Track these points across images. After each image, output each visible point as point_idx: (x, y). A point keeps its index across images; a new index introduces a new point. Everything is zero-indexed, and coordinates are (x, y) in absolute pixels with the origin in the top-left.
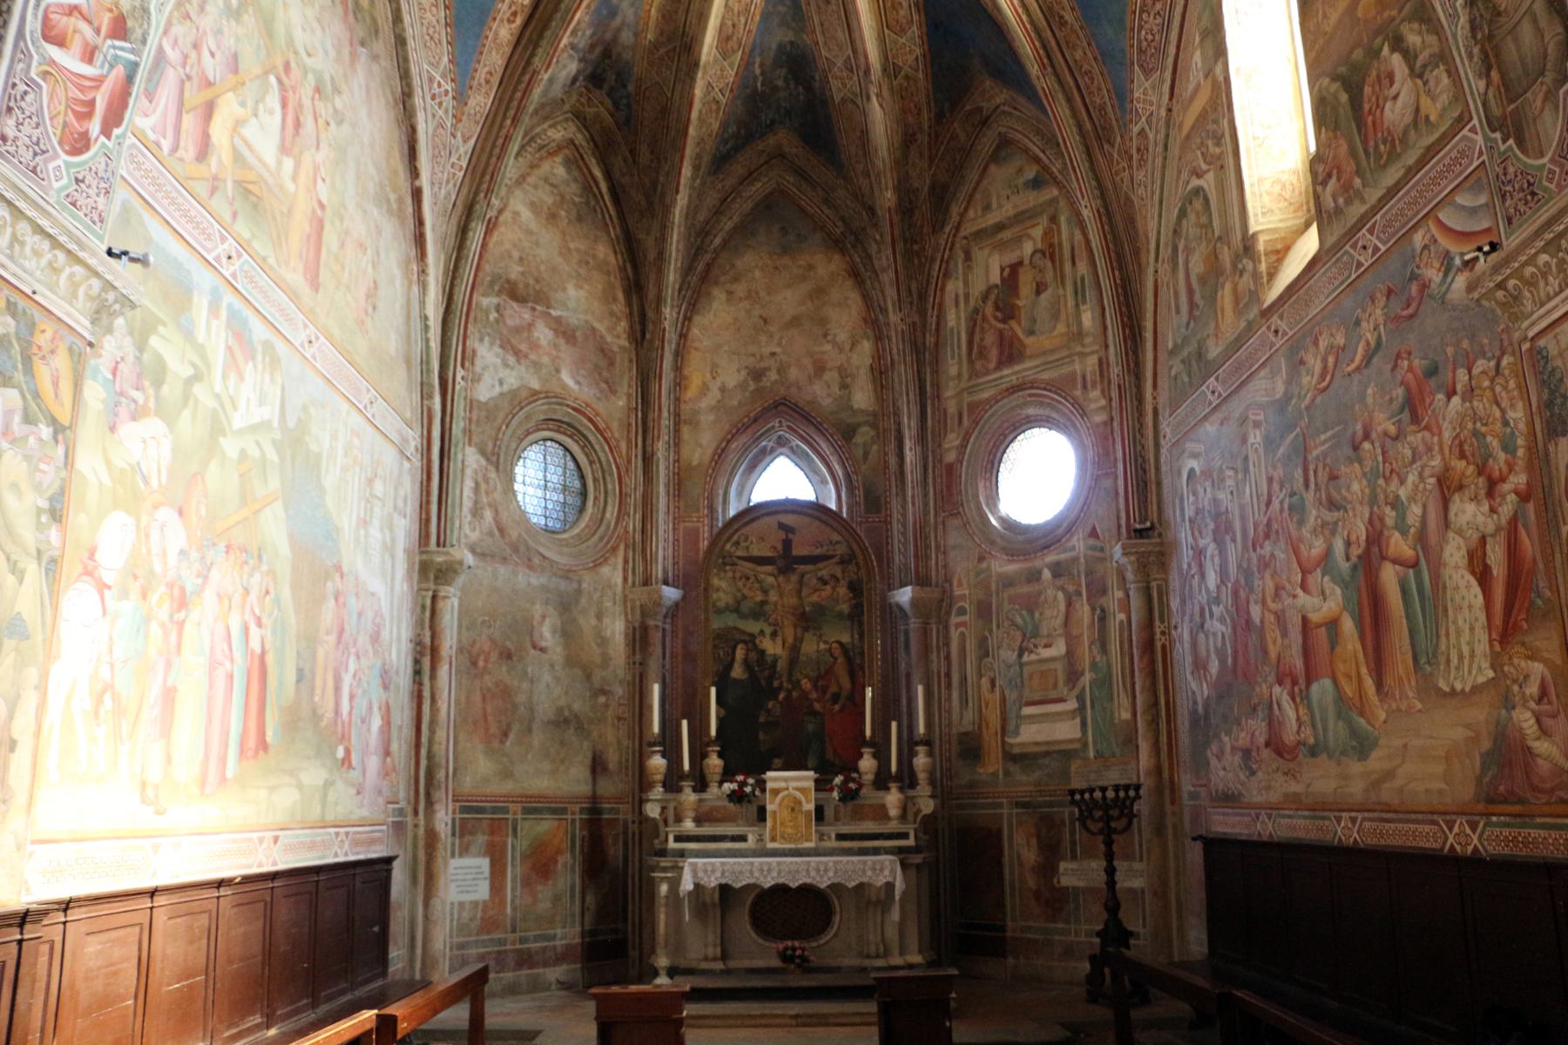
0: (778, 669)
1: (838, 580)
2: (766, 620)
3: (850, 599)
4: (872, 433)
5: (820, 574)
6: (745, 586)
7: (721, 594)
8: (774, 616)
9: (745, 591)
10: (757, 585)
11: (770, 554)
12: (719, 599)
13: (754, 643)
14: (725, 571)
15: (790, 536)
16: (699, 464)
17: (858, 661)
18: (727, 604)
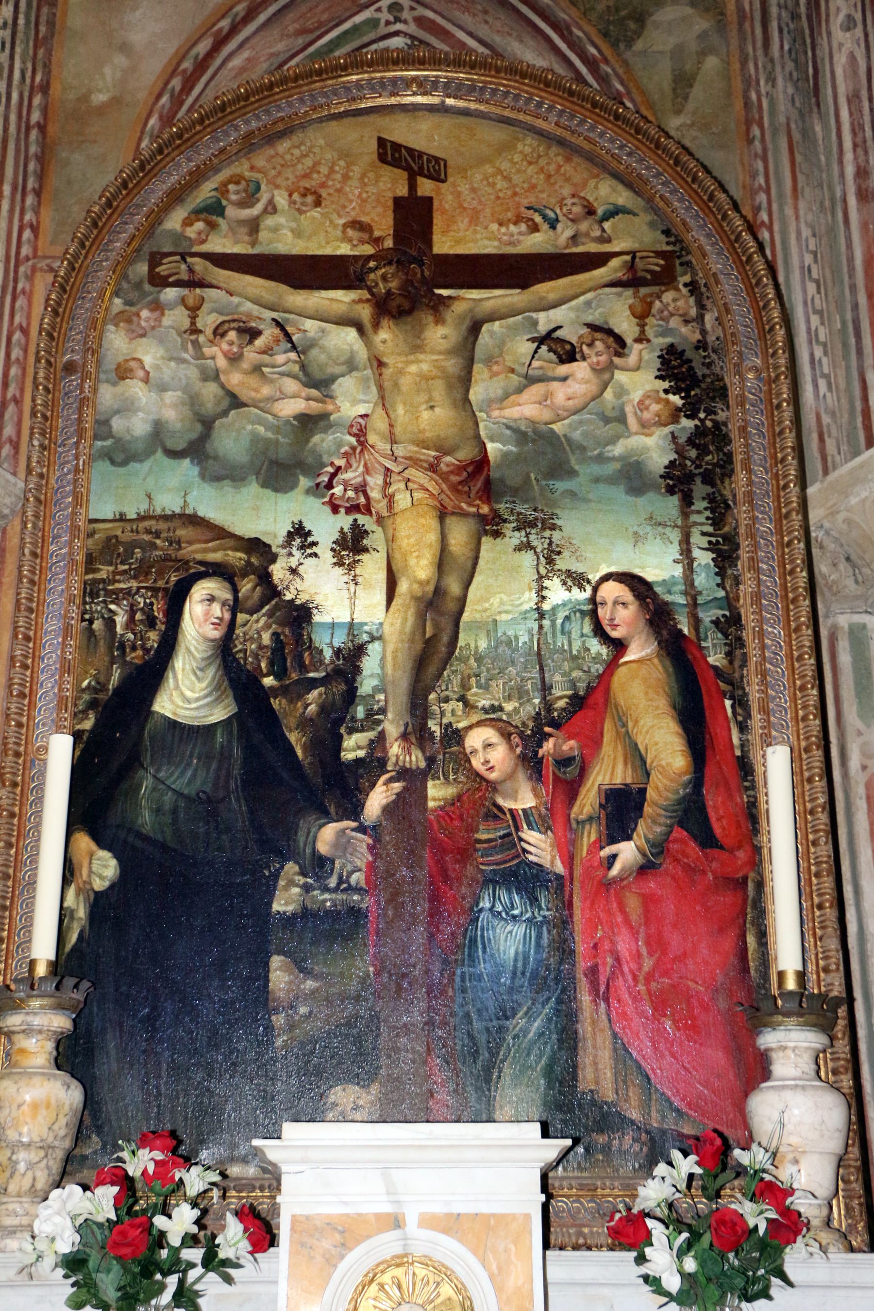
0: (366, 685)
1: (620, 341)
2: (316, 490)
3: (675, 415)
4: (702, 24)
5: (545, 321)
6: (234, 359)
7: (136, 389)
8: (352, 476)
9: (235, 379)
10: (284, 358)
11: (344, 249)
12: (127, 408)
13: (265, 578)
14: (158, 307)
15: (425, 187)
16: (116, 102)
17: (716, 658)
18: (158, 430)
